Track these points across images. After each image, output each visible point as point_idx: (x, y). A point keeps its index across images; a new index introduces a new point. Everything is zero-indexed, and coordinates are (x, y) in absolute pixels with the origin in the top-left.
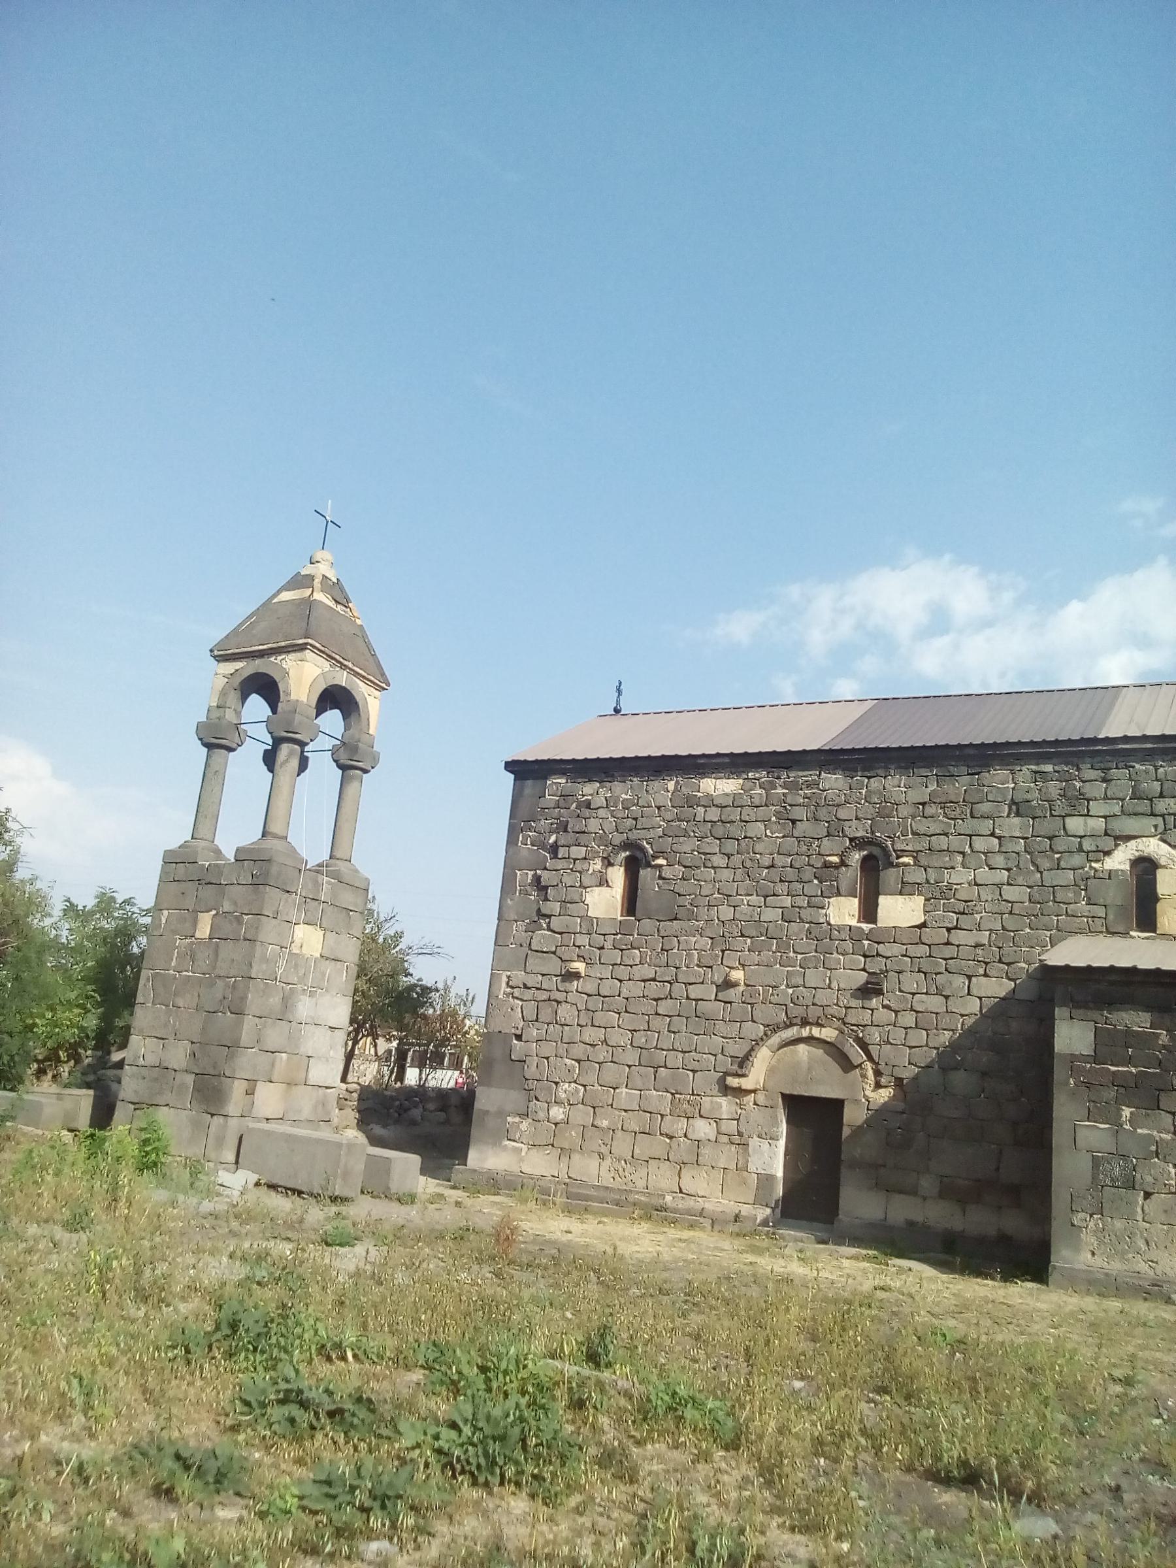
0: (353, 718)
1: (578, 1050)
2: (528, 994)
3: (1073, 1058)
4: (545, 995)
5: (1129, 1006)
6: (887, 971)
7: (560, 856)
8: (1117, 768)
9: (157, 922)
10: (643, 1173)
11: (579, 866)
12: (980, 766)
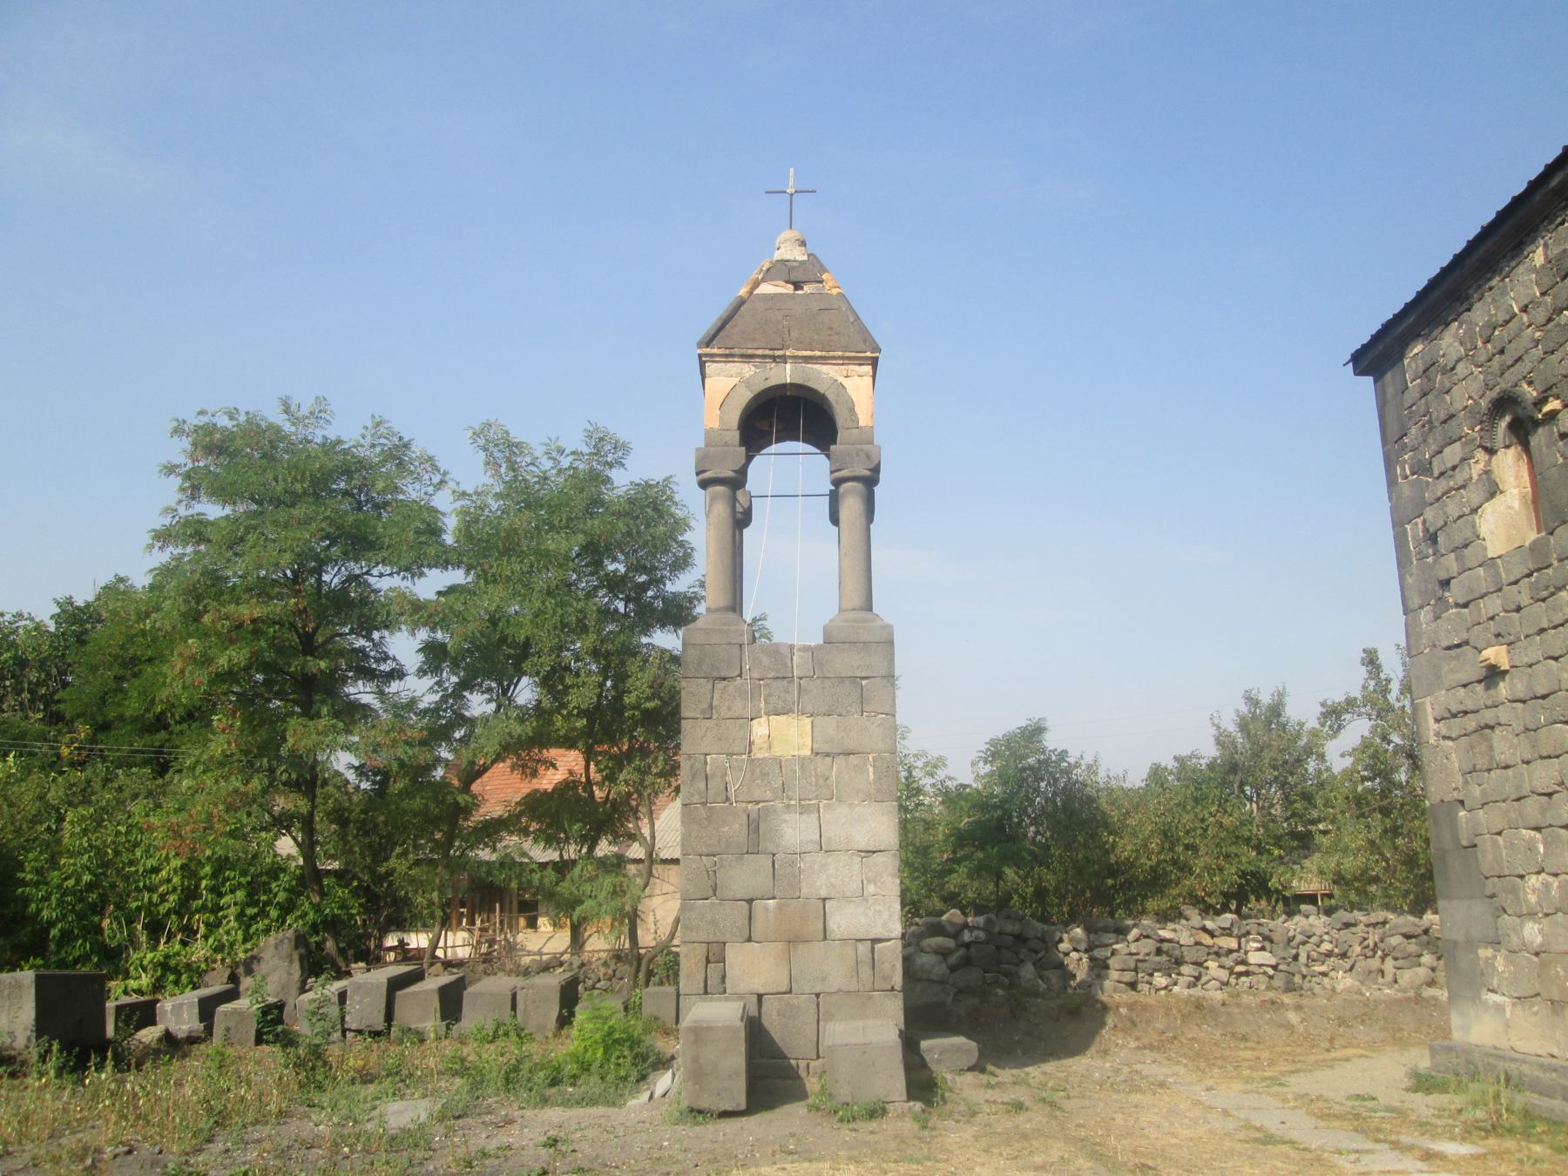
4: (1471, 723)
11: (1460, 477)
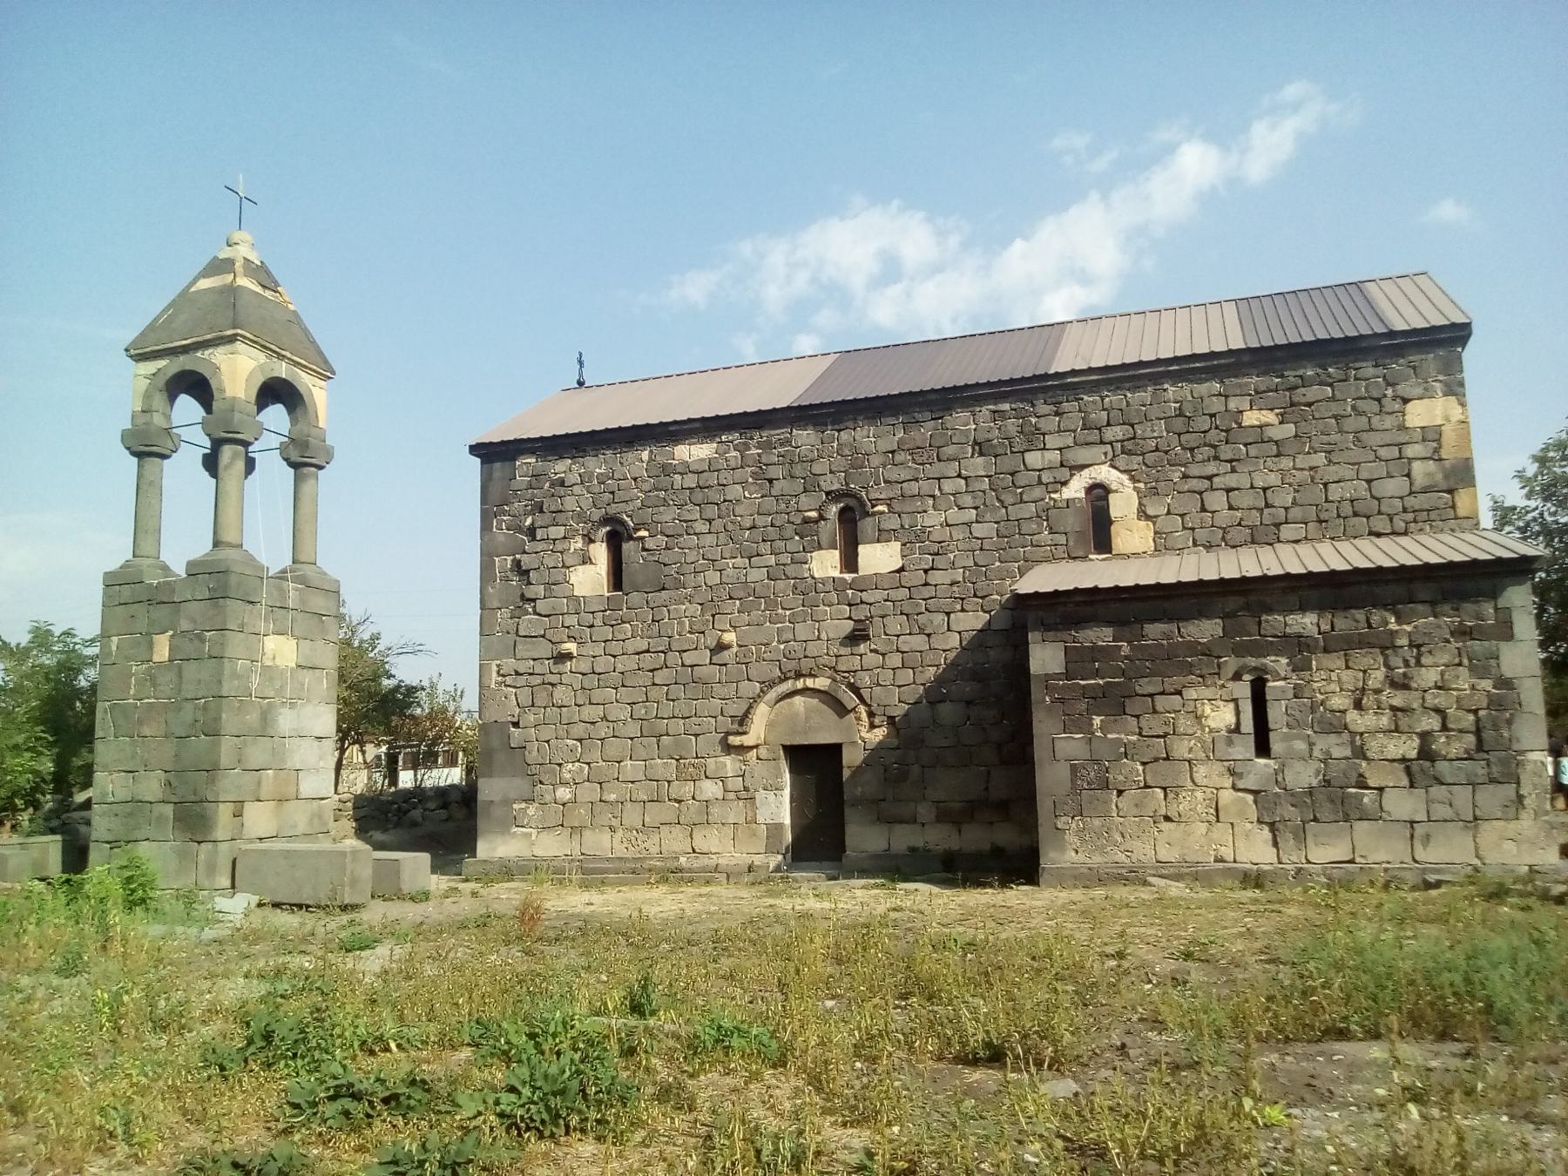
0: (299, 411)
1: (579, 730)
2: (521, 681)
3: (1048, 677)
4: (537, 680)
5: (1092, 624)
6: (872, 617)
7: (538, 538)
8: (1067, 401)
9: (107, 651)
10: (656, 839)
11: (559, 546)
12: (943, 410)
